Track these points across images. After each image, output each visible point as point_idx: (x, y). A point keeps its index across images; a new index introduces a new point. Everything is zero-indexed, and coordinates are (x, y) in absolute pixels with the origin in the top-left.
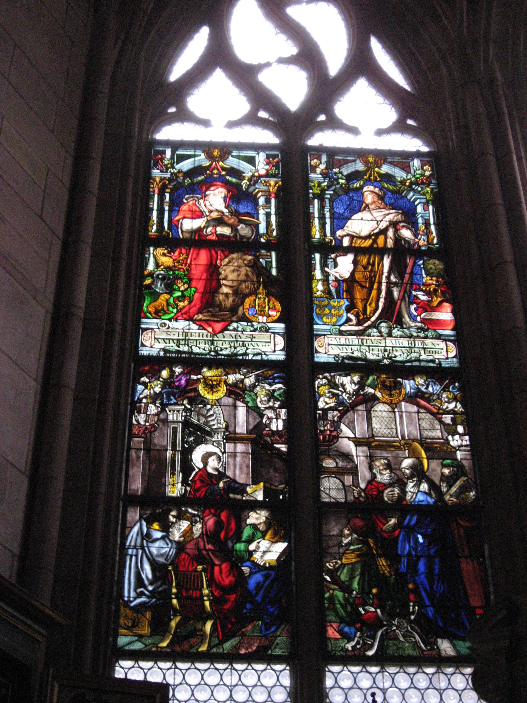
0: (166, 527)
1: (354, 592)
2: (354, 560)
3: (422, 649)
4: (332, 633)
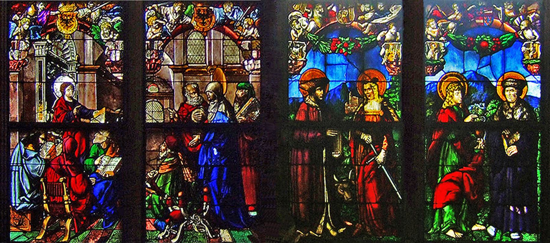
0: (37, 148)
1: (166, 196)
2: (167, 170)
3: (209, 238)
4: (150, 226)
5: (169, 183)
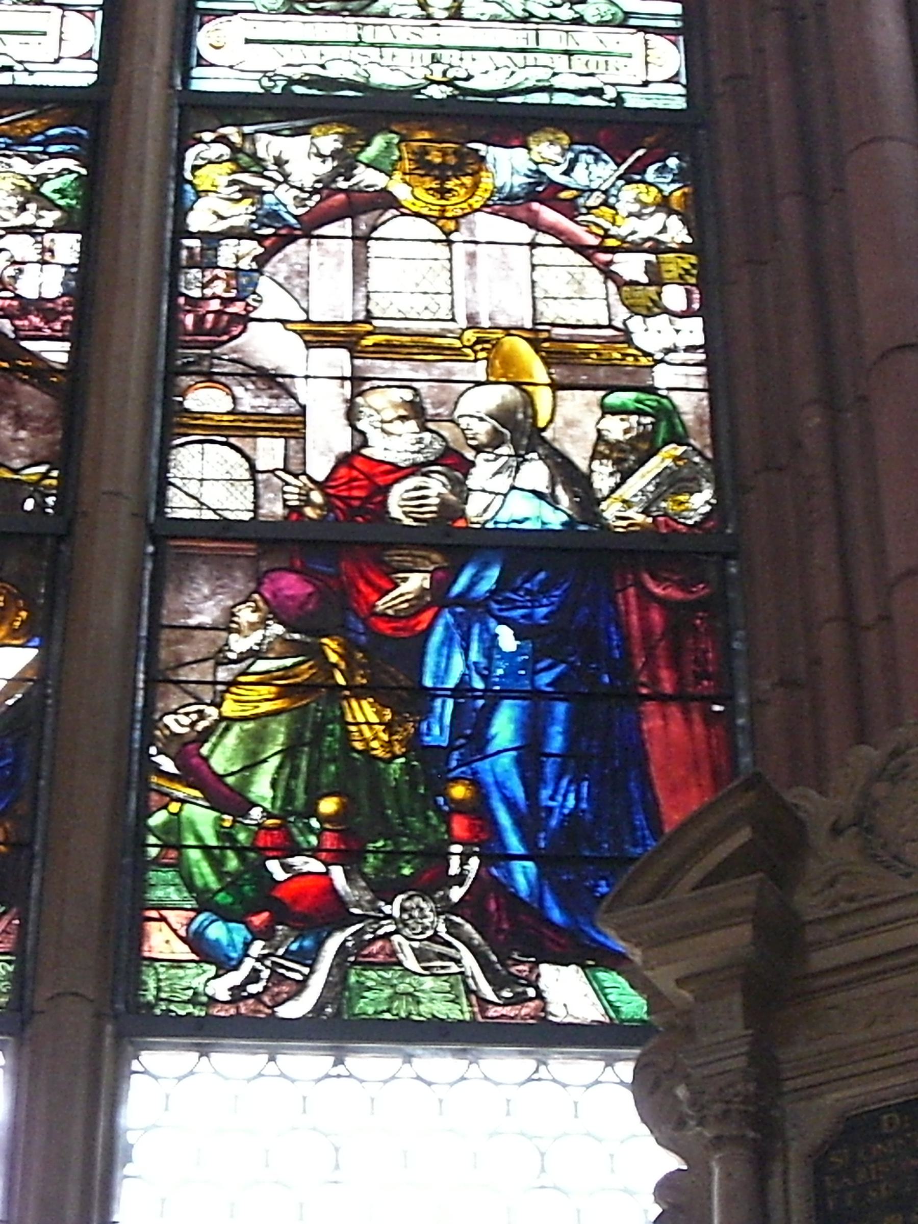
1: (256, 813)
3: (484, 1002)
4: (161, 941)
5: (275, 761)
